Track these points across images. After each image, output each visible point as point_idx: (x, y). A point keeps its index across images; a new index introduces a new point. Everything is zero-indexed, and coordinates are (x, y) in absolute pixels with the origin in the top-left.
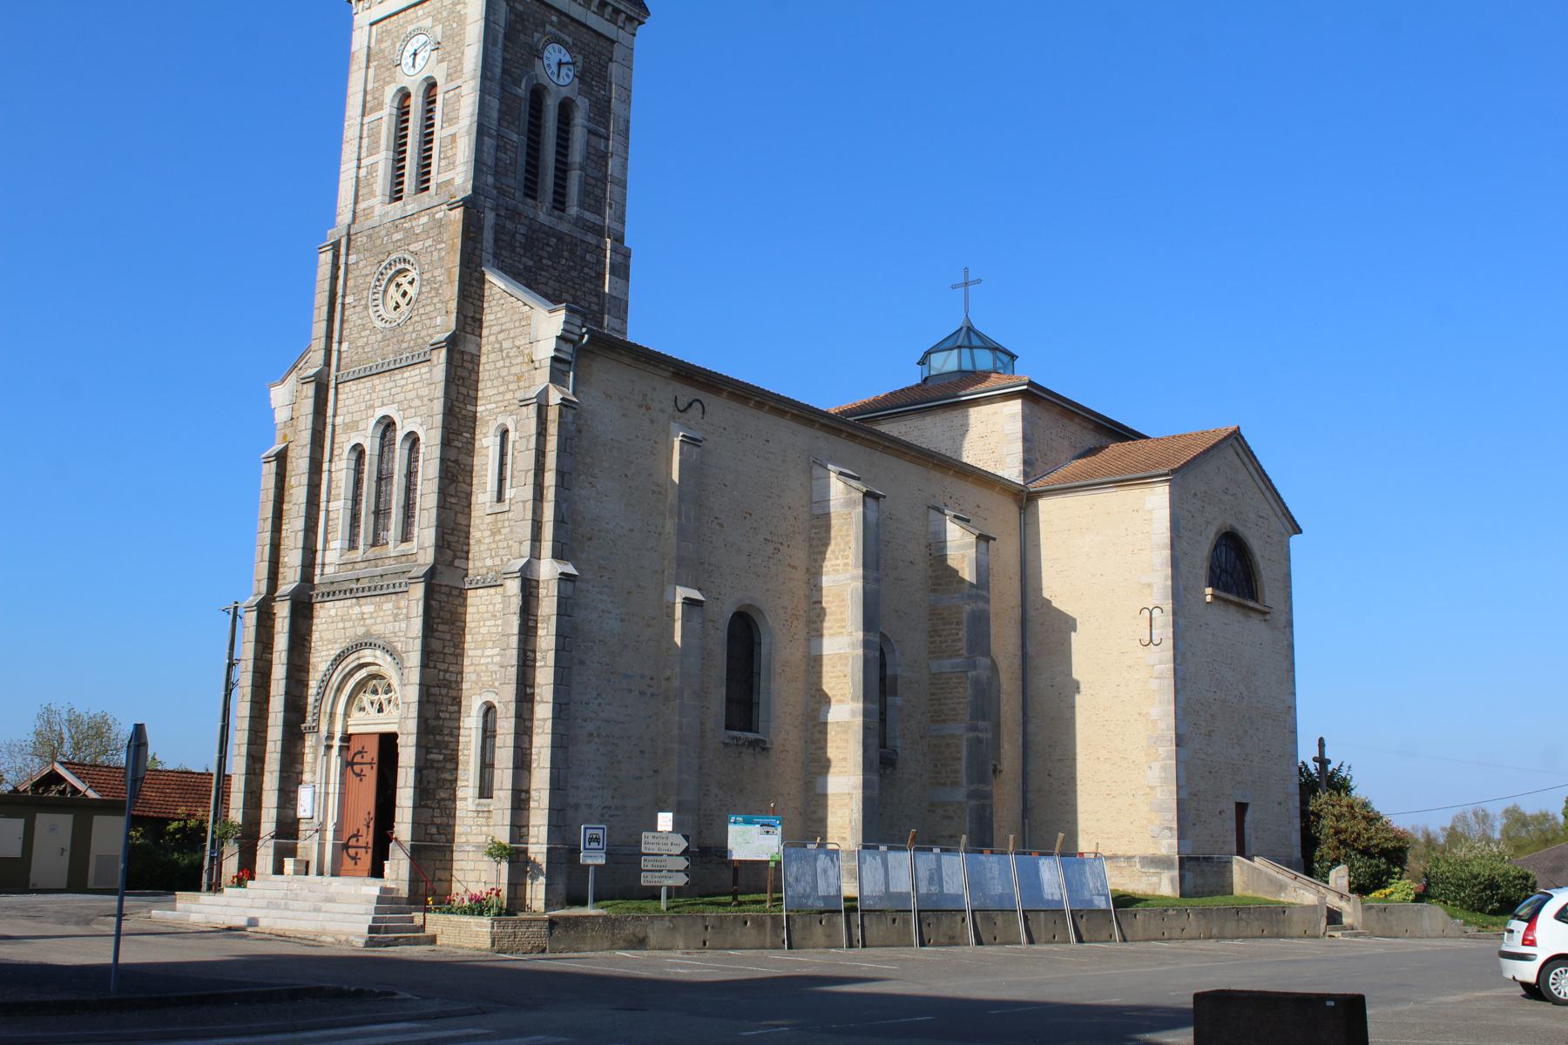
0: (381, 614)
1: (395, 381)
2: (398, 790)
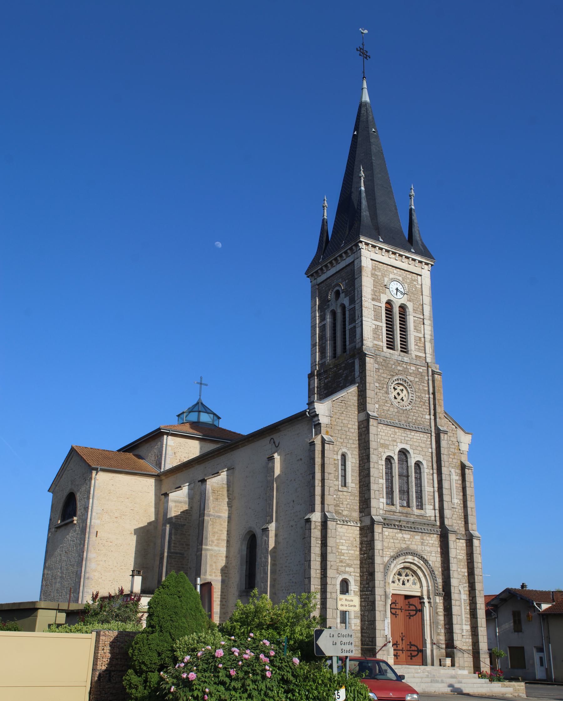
0: (415, 540)
1: (407, 434)
2: (454, 625)
